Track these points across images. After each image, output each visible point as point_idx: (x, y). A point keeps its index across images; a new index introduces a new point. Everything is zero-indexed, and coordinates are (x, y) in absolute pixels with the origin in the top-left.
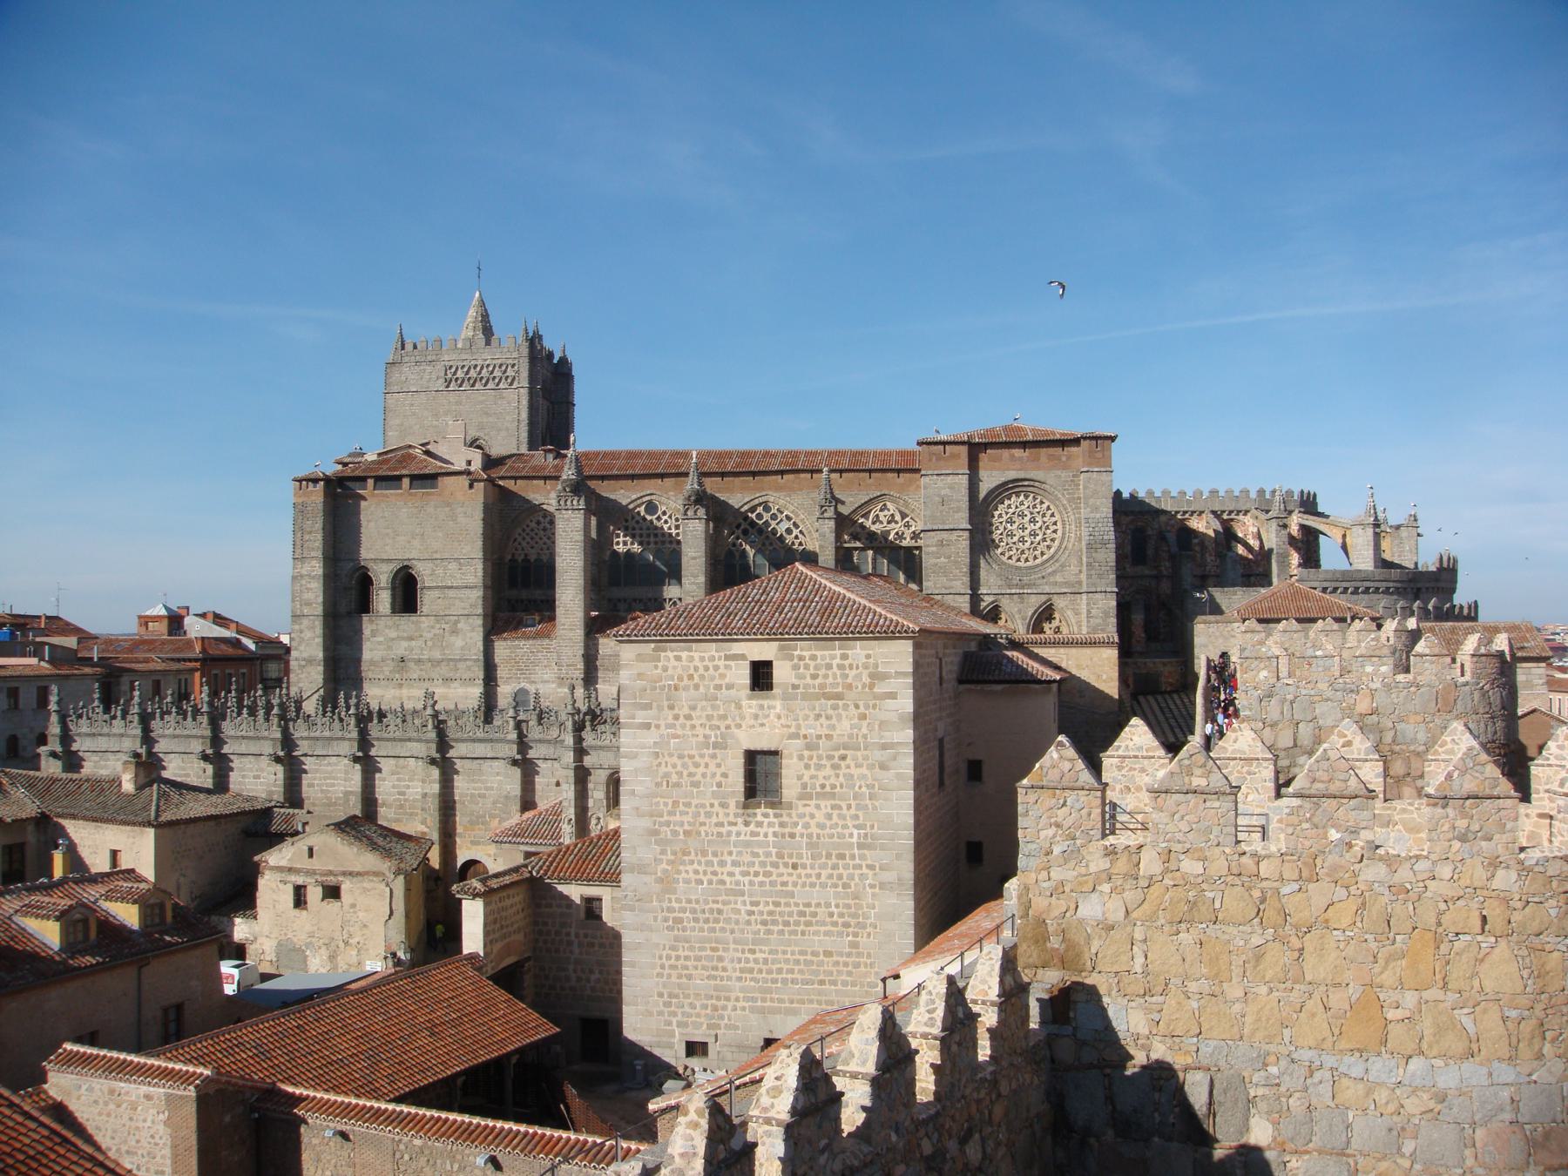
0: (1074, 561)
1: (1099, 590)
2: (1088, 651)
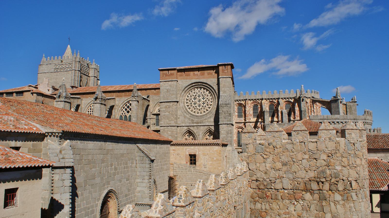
1: (224, 123)
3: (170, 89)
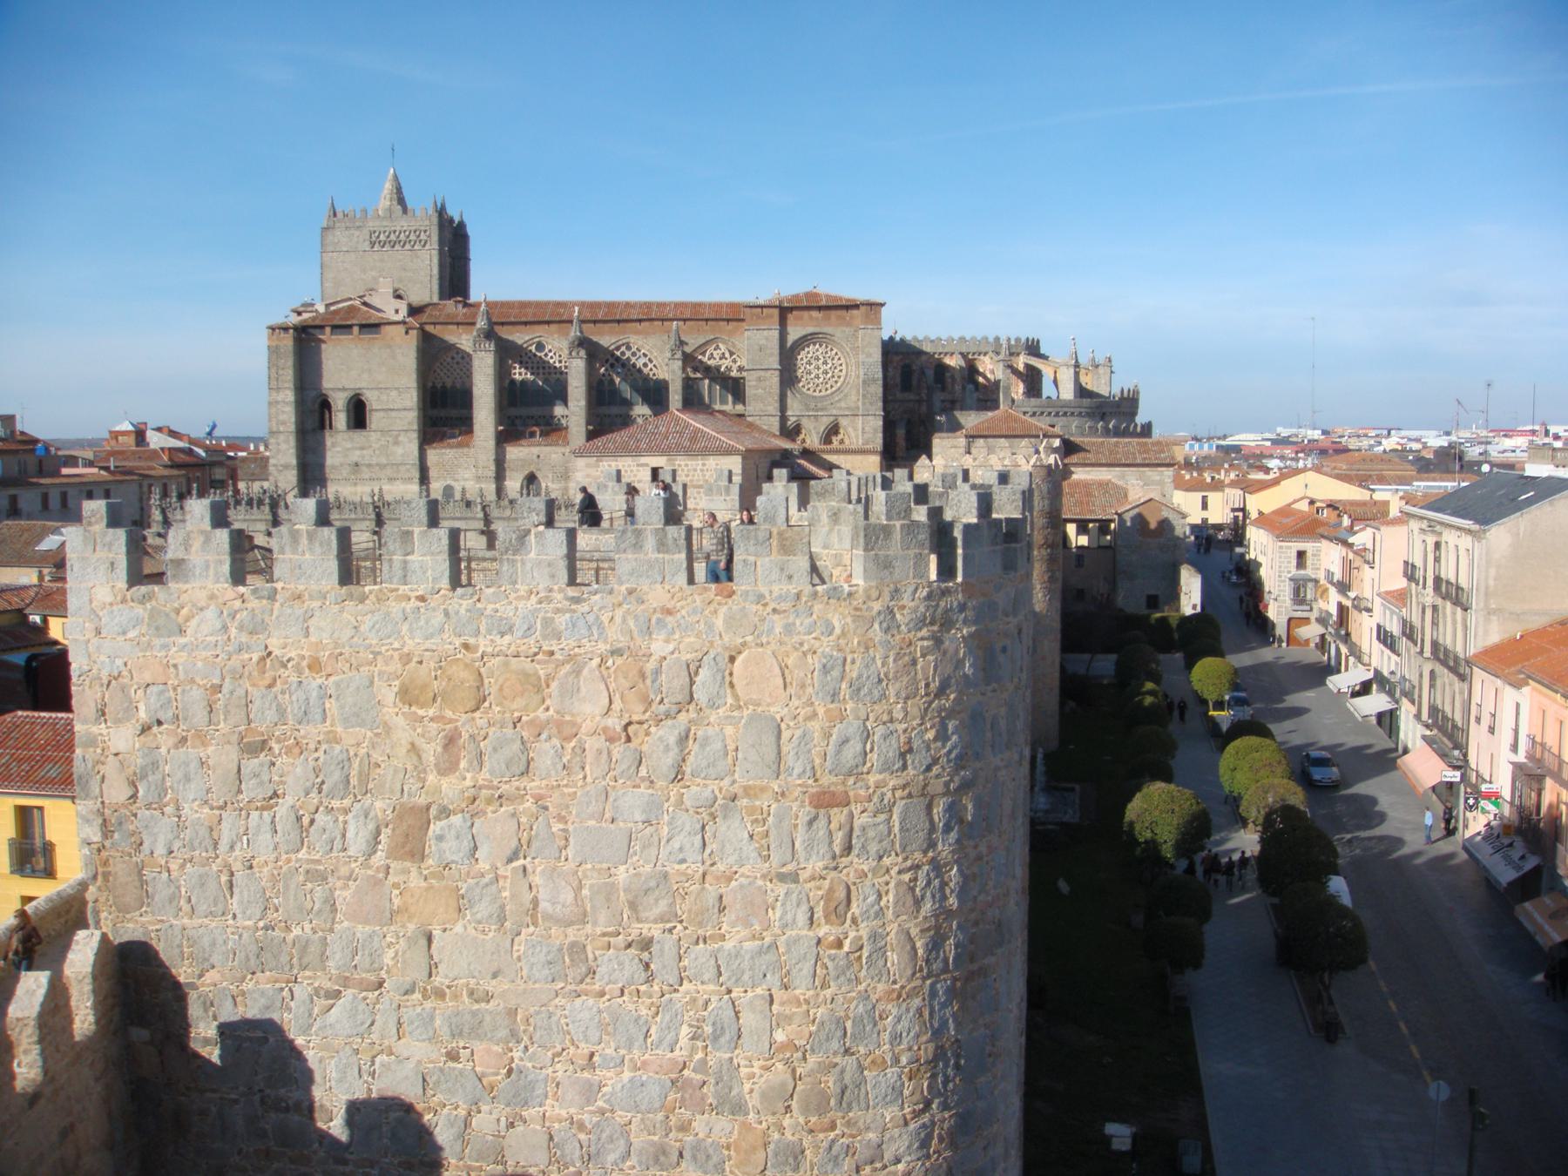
0: (854, 392)
2: (859, 457)
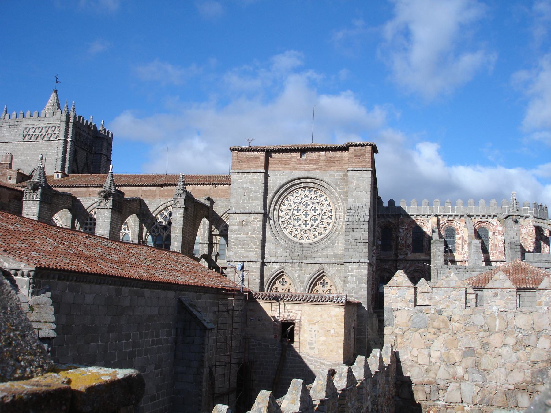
1: (354, 261)
3: (251, 189)
